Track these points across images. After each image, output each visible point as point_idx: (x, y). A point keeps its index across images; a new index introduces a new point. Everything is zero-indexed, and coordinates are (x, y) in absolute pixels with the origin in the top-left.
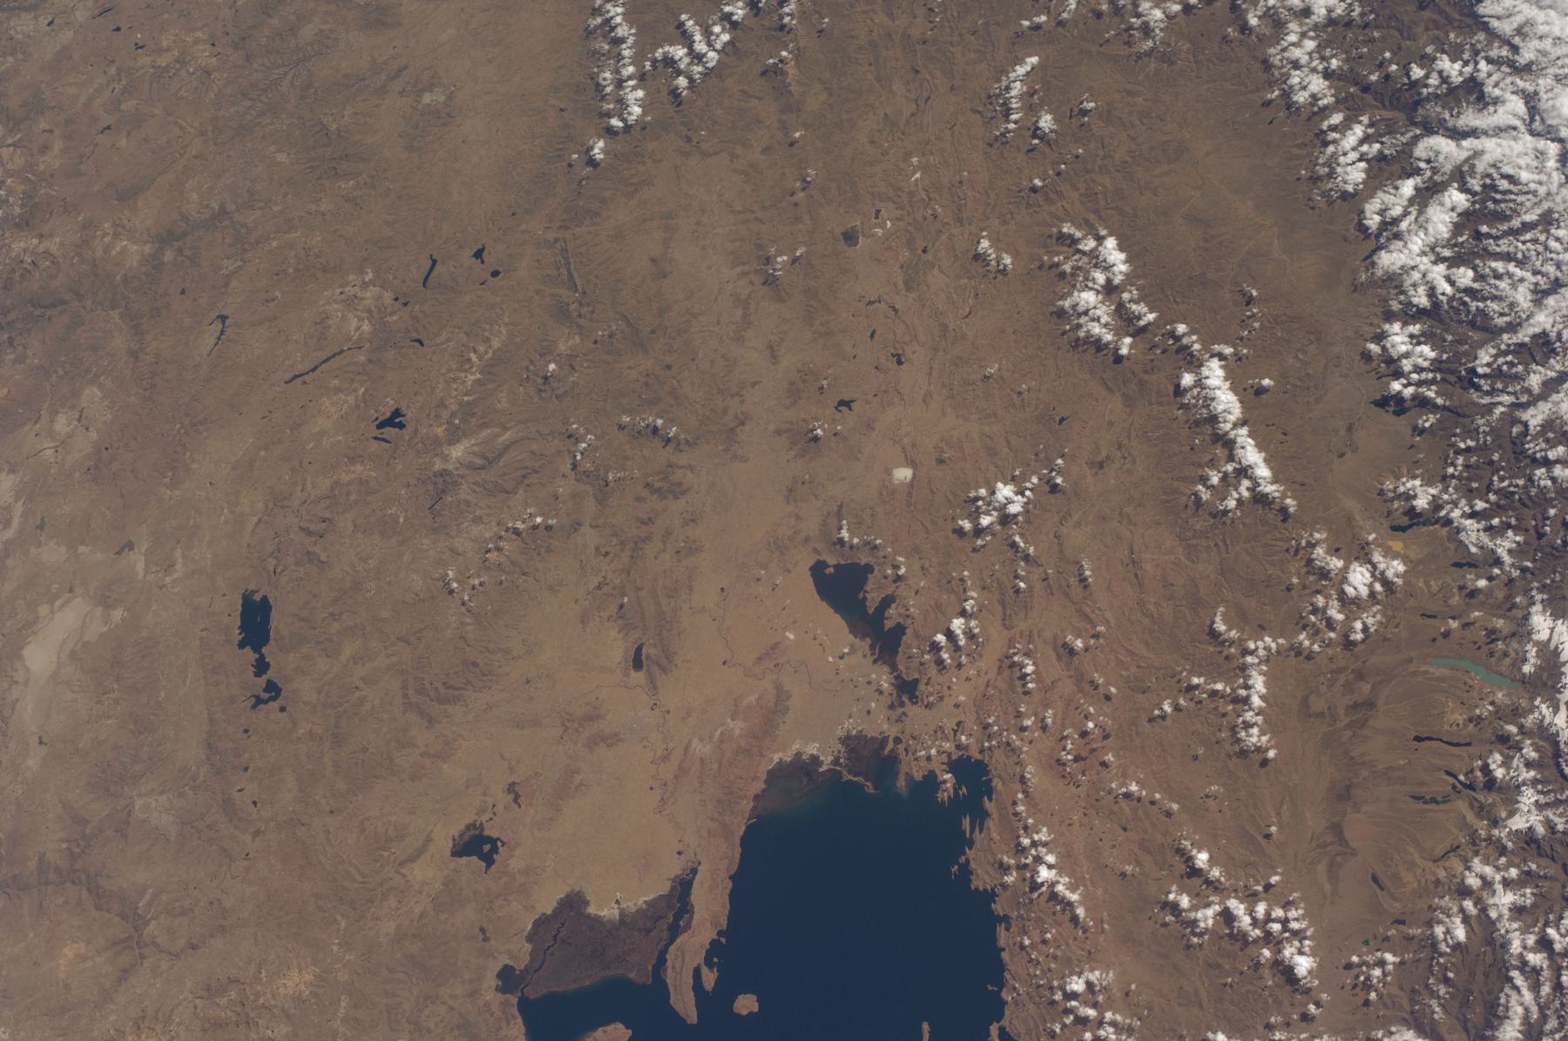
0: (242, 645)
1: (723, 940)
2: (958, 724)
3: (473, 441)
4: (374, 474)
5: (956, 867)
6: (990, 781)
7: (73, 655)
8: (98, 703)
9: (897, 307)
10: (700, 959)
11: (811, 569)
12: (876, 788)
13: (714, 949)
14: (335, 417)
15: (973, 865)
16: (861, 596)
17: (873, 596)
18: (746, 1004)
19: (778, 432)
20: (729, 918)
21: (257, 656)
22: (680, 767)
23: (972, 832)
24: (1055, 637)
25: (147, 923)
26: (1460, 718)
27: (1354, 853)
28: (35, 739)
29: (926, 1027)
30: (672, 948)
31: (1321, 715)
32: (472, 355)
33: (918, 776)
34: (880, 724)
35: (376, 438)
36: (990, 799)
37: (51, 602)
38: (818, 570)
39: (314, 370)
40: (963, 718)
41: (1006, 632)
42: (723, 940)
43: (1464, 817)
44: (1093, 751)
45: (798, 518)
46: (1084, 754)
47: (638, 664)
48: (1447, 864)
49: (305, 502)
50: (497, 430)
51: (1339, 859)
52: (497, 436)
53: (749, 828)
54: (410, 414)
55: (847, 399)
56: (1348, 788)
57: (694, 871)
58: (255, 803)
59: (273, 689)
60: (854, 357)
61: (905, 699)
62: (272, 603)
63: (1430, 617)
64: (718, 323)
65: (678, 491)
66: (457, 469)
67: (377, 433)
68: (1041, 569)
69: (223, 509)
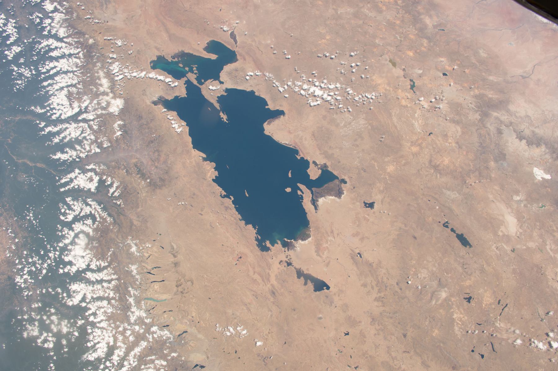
0: (462, 235)
1: (301, 200)
2: (272, 259)
3: (442, 298)
4: (462, 283)
5: (257, 227)
6: (259, 248)
7: (504, 222)
8: (486, 212)
9: (349, 367)
10: (304, 195)
11: (330, 287)
12: (284, 240)
13: (302, 198)
14: (485, 297)
15: (253, 229)
16: (313, 284)
17: (310, 285)
18: (288, 190)
19: (360, 322)
20: (302, 205)
21: (456, 233)
22: (333, 233)
23: (257, 236)
24: (259, 285)
25: (434, 172)
26: (156, 287)
27: (169, 252)
28: (494, 200)
29: (247, 195)
30: (311, 195)
31: (188, 281)
32: (460, 323)
33: (276, 245)
34: (291, 252)
35: (469, 293)
36: (256, 244)
37: (521, 233)
38: (328, 288)
39: (503, 310)
40: (272, 260)
41: (272, 283)
42: (301, 200)
43: (147, 265)
44: (238, 260)
45: (341, 299)
46: (239, 259)
47: (359, 253)
48: (148, 254)
49: (475, 272)
50: (437, 303)
51: (172, 250)
52: (436, 302)
53: (309, 224)
54: (465, 302)
55: (347, 335)
56: (175, 266)
57: (316, 212)
58: (429, 201)
59: (447, 227)
60: (352, 348)
61: (289, 261)
62: (463, 246)
63: (170, 311)
64: (397, 350)
65: (377, 299)
66: (440, 290)
67: (470, 295)
68: (271, 301)
69: (496, 266)
